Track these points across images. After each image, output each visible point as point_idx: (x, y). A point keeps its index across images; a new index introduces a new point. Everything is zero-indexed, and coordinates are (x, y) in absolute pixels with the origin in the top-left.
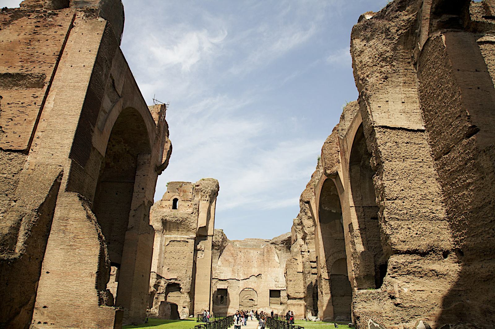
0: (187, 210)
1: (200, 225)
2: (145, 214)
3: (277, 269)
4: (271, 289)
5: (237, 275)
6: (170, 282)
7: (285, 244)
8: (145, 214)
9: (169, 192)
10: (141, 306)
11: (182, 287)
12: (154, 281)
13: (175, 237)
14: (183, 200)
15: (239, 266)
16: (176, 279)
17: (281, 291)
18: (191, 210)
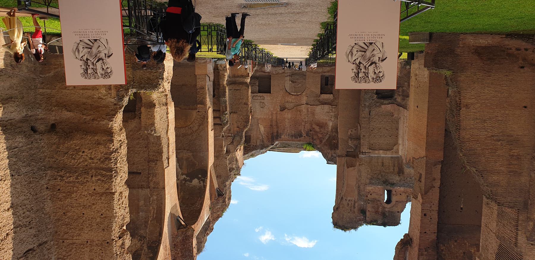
0: (373, 188)
1: (354, 169)
2: (420, 182)
3: (262, 117)
4: (269, 94)
5: (309, 110)
7: (252, 146)
8: (420, 182)
9: (398, 212)
10: (417, 72)
11: (375, 95)
13: (386, 154)
14: (379, 202)
15: (306, 120)
16: (382, 104)
17: (257, 92)
18: (368, 188)
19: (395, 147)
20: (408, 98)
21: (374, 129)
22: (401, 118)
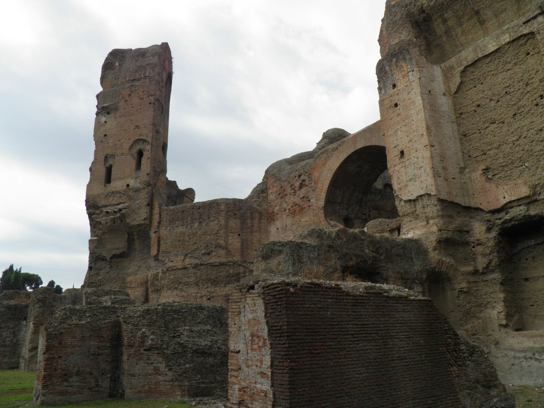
6: (508, 217)
12: (435, 229)
19: (458, 84)
20: (445, 236)
21: (537, 105)
22: (459, 170)
